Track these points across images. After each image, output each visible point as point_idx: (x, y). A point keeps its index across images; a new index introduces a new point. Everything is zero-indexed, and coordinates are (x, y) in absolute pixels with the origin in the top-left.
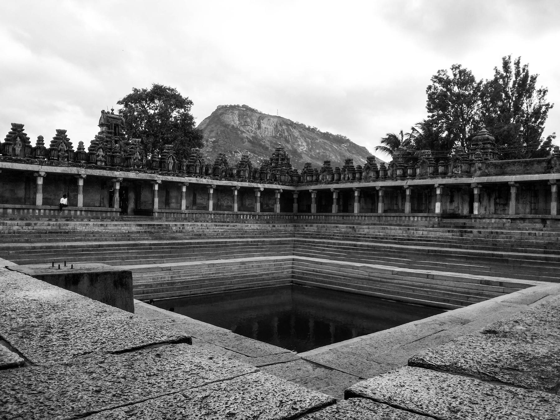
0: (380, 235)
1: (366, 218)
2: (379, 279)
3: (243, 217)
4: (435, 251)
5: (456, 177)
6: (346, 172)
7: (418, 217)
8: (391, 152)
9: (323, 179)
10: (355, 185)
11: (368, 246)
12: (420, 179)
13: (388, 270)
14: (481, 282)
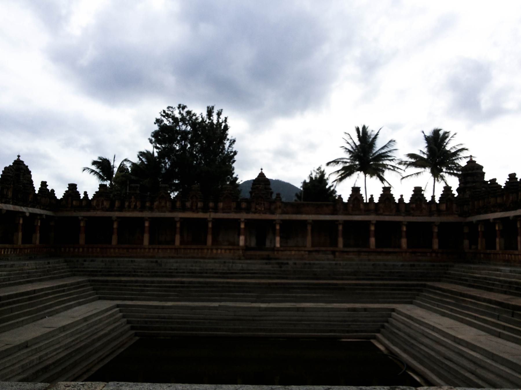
0: (195, 269)
1: (160, 251)
2: (251, 318)
3: (4, 252)
4: (276, 284)
5: (260, 213)
6: (133, 200)
7: (221, 249)
8: (100, 177)
9: (98, 205)
10: (146, 214)
11: (199, 283)
12: (224, 213)
13: (254, 308)
14: (349, 310)
